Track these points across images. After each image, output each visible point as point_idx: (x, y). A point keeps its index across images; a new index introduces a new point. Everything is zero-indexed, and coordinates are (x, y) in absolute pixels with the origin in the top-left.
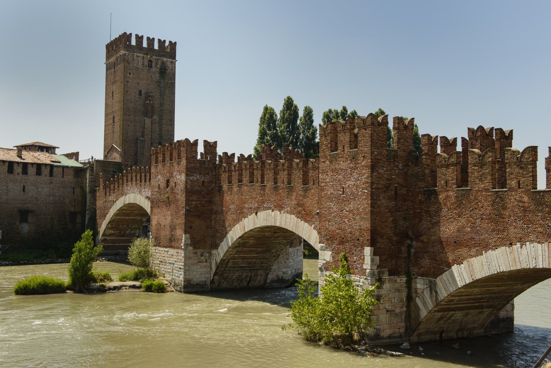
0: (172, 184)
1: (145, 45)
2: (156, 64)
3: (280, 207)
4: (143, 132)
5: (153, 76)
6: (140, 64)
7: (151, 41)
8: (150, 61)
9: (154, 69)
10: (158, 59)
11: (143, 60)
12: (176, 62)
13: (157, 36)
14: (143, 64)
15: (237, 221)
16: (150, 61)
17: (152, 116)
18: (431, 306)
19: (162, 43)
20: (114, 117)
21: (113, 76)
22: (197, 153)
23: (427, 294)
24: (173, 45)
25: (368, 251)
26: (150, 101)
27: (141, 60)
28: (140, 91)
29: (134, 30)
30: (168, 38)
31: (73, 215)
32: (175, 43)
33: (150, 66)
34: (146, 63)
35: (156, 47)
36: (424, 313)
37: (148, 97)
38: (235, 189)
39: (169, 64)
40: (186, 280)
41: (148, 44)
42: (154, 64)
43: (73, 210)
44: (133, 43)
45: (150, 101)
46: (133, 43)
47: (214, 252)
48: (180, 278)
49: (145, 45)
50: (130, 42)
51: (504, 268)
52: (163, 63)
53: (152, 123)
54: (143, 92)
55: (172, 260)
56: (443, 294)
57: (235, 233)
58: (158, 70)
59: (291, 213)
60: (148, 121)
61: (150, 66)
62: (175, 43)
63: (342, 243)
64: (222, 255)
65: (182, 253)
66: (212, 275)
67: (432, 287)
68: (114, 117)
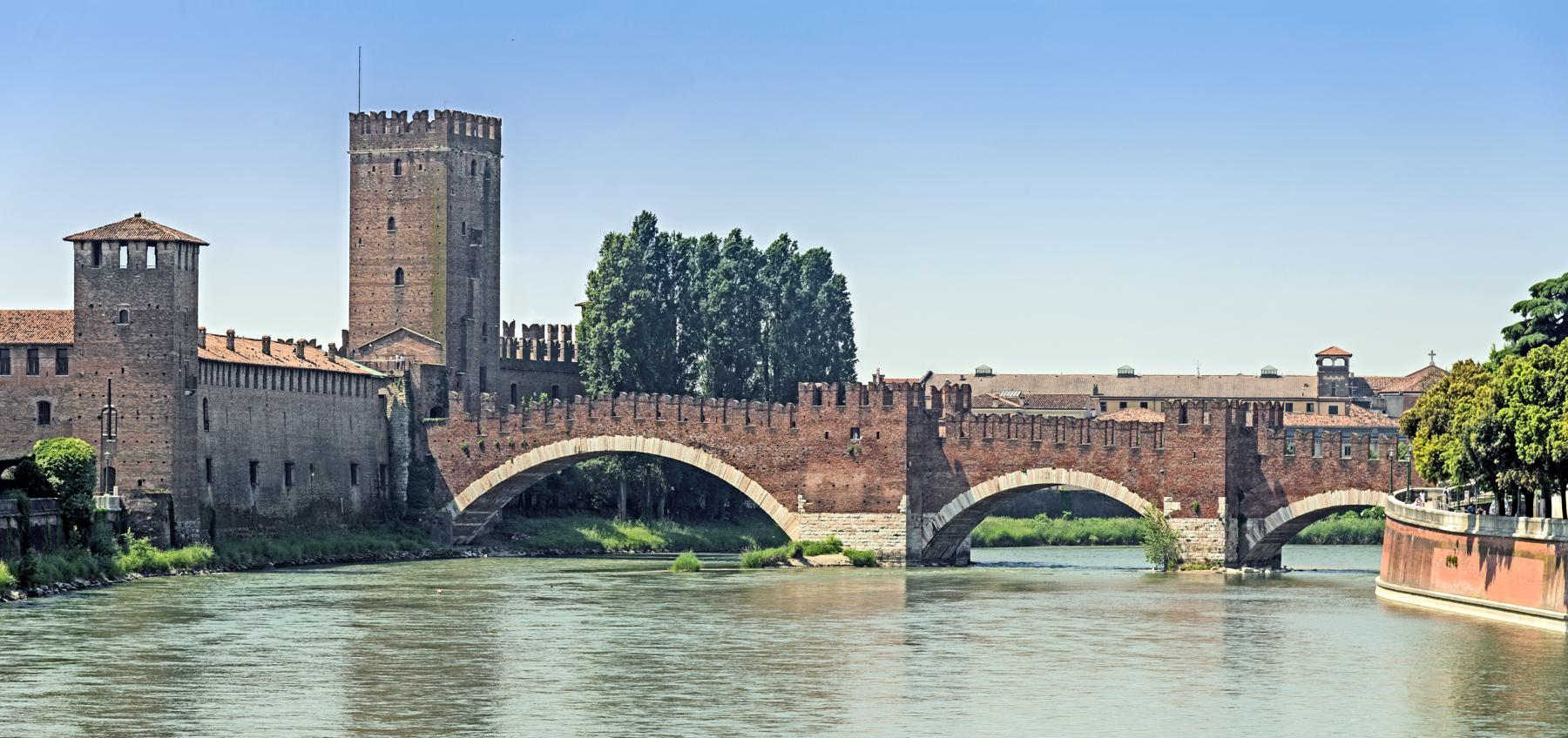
0: (867, 432)
3: (1068, 465)
4: (470, 305)
15: (983, 479)
18: (1259, 538)
20: (399, 272)
21: (389, 186)
23: (1256, 531)
24: (498, 123)
25: (1222, 500)
31: (382, 466)
36: (1253, 544)
38: (978, 443)
40: (908, 549)
43: (381, 459)
47: (931, 515)
48: (901, 545)
51: (1319, 507)
55: (871, 527)
56: (1270, 528)
57: (980, 492)
59: (1086, 470)
61: (473, 173)
63: (1193, 494)
64: (948, 519)
65: (904, 518)
66: (925, 544)
67: (1261, 526)
68: (399, 272)
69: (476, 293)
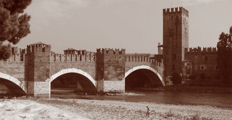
7: (172, 9)
8: (172, 16)
9: (173, 19)
13: (174, 7)
22: (181, 48)
27: (169, 17)
28: (169, 28)
29: (166, 8)
33: (172, 18)
34: (171, 17)
35: (174, 11)
39: (179, 16)
41: (171, 11)
42: (173, 17)
45: (171, 31)
58: (175, 19)
60: (171, 38)
61: (172, 18)
69: (170, 41)
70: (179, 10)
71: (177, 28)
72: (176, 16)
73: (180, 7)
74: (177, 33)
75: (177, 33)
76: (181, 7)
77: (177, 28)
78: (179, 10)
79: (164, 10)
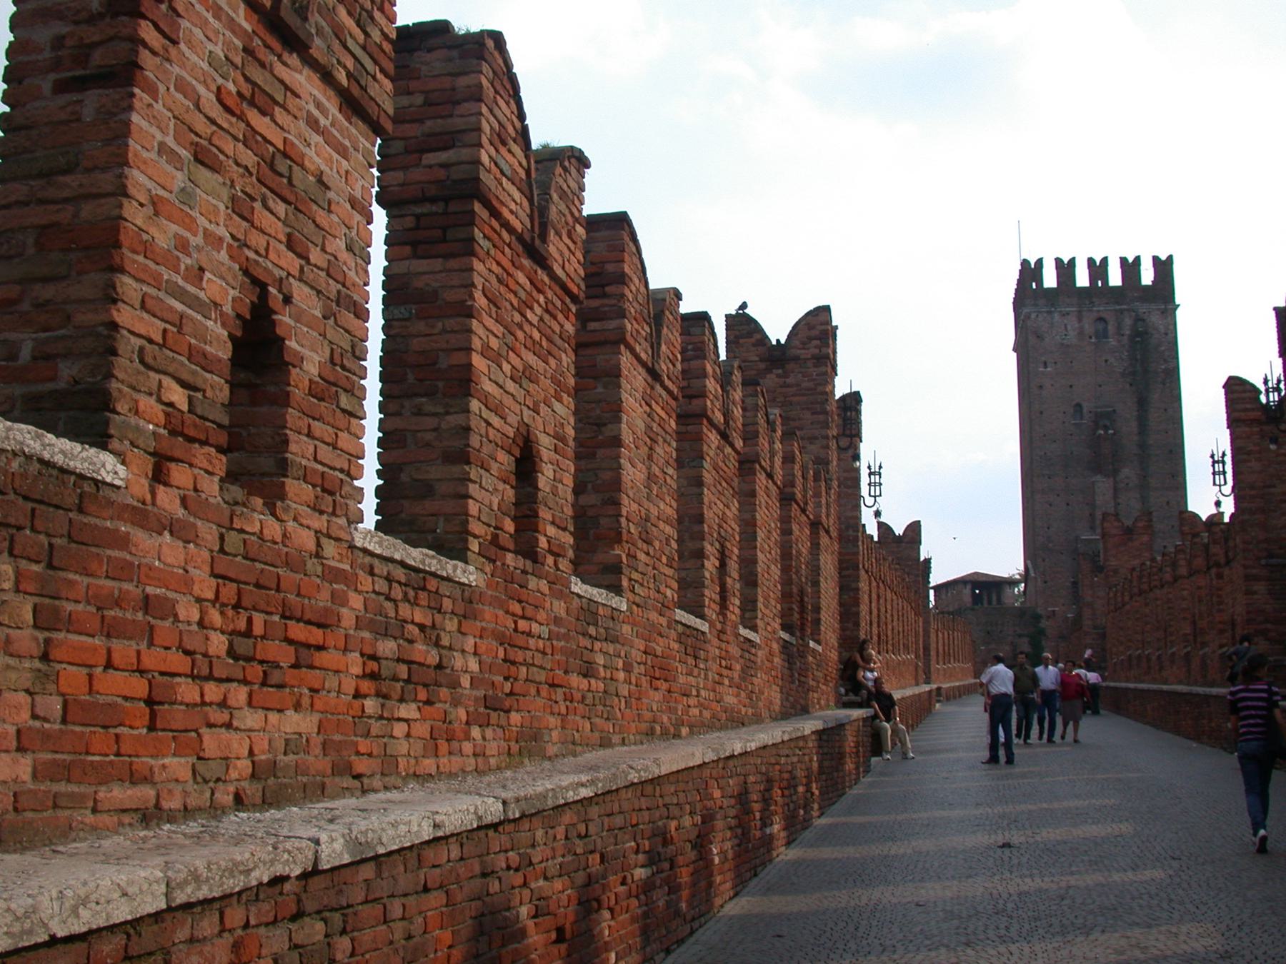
1: (1082, 279)
2: (1119, 327)
5: (1112, 360)
6: (1072, 334)
7: (1098, 269)
9: (1112, 342)
10: (1122, 311)
11: (1080, 320)
12: (1178, 312)
13: (1114, 251)
14: (1081, 333)
16: (1101, 319)
17: (1115, 472)
19: (1130, 268)
26: (1106, 428)
27: (1072, 322)
28: (1079, 405)
29: (1048, 251)
30: (1146, 251)
32: (1170, 258)
34: (1088, 327)
35: (1115, 278)
37: (1104, 418)
39: (1155, 319)
41: (1092, 279)
44: (1050, 279)
45: (1106, 428)
46: (1050, 279)
49: (1082, 279)
50: (1039, 280)
52: (1138, 319)
53: (1116, 490)
54: (1085, 410)
58: (1125, 340)
60: (1103, 486)
62: (1170, 258)
70: (1147, 277)
71: (1142, 403)
72: (1128, 322)
73: (1155, 259)
74: (1143, 446)
75: (1143, 446)
76: (1163, 258)
77: (1142, 403)
78: (1147, 277)
79: (1030, 272)
